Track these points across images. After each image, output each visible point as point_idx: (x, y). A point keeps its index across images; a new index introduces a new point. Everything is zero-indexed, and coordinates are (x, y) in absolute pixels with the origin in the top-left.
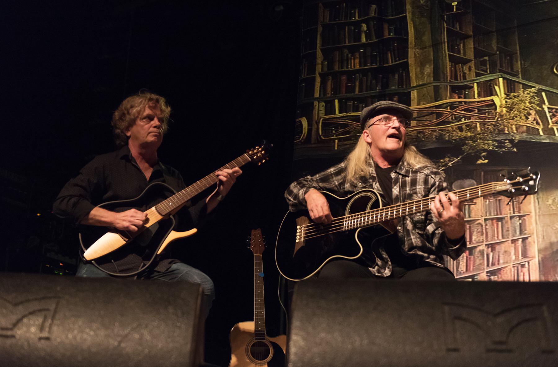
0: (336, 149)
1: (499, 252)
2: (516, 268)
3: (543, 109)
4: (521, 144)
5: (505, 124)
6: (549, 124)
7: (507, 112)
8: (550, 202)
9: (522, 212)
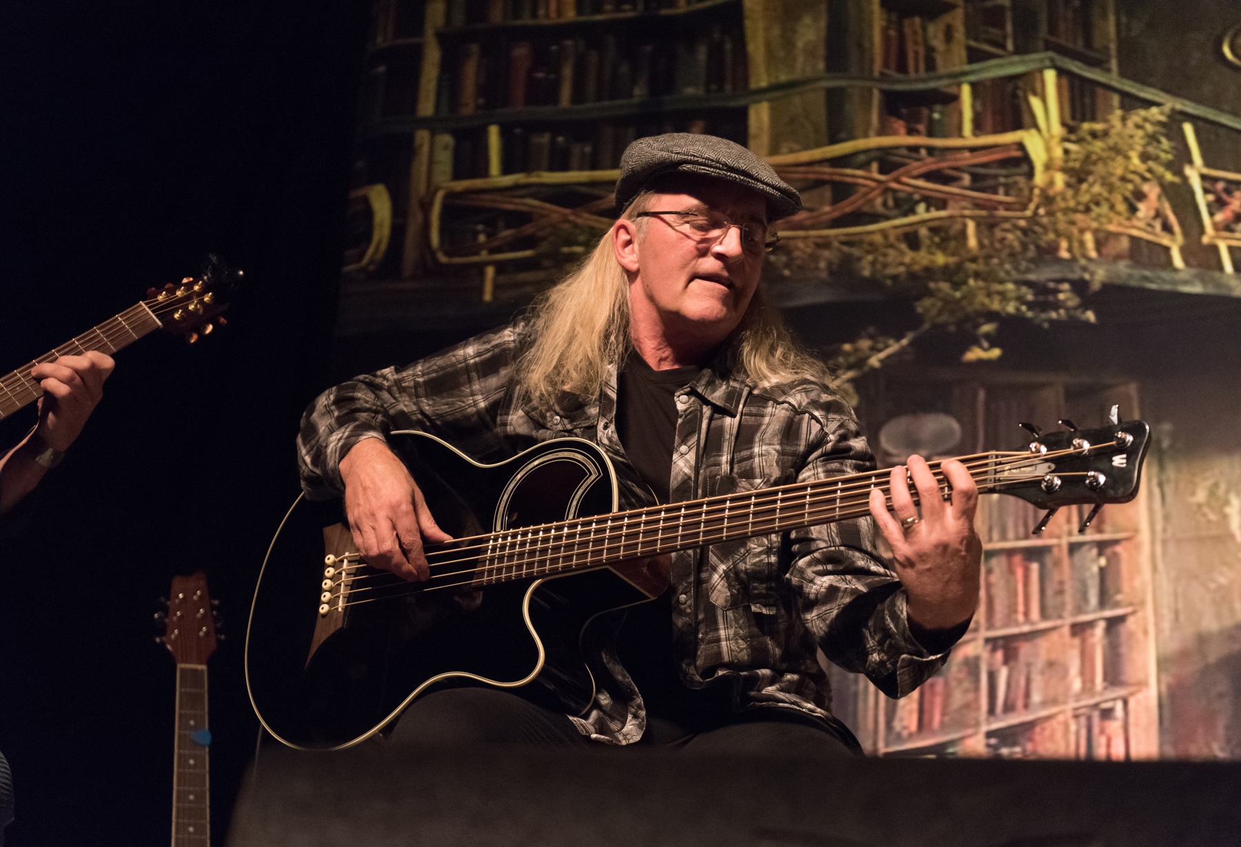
0: (488, 297)
1: (1029, 665)
2: (1083, 720)
3: (1185, 179)
4: (1112, 298)
5: (1062, 226)
6: (1202, 230)
7: (1068, 185)
8: (1201, 496)
9: (1107, 527)
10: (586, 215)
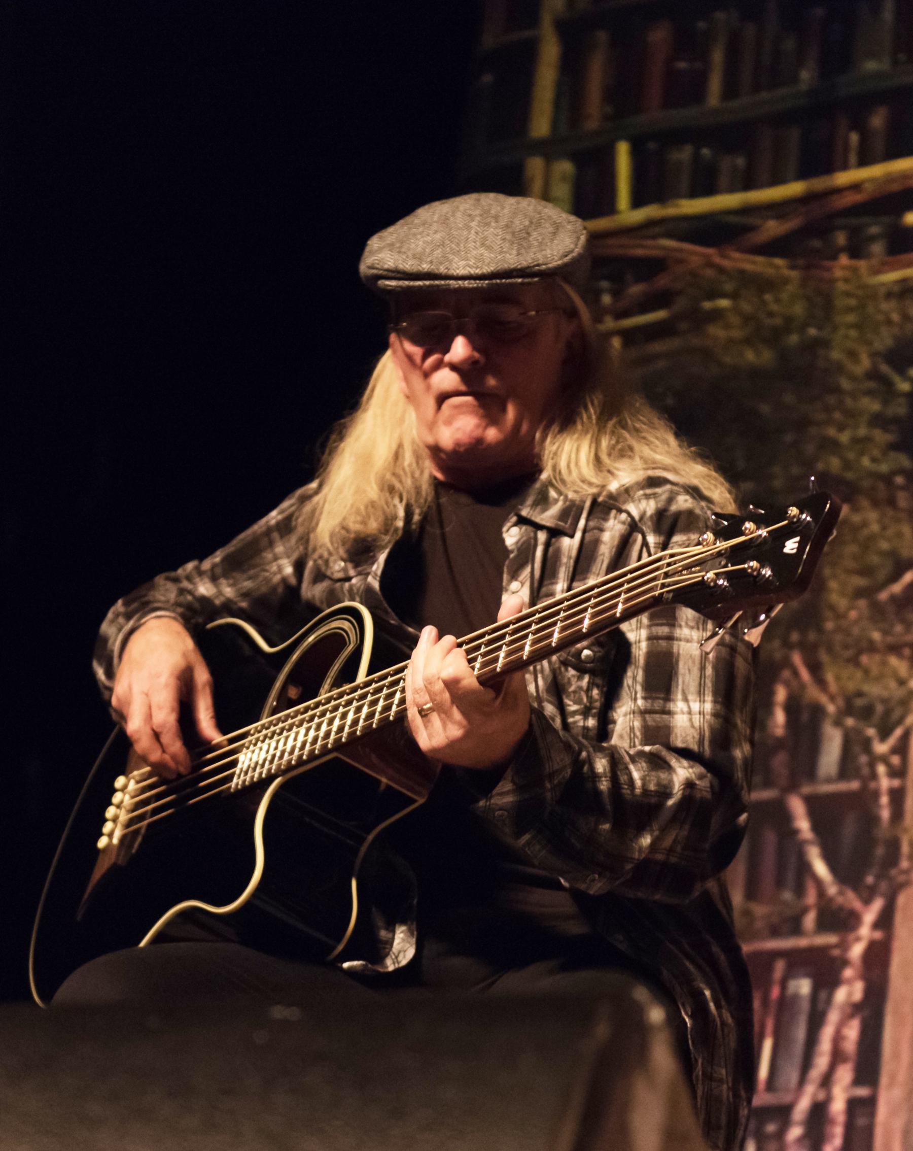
10: (737, 255)
